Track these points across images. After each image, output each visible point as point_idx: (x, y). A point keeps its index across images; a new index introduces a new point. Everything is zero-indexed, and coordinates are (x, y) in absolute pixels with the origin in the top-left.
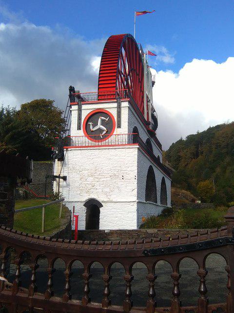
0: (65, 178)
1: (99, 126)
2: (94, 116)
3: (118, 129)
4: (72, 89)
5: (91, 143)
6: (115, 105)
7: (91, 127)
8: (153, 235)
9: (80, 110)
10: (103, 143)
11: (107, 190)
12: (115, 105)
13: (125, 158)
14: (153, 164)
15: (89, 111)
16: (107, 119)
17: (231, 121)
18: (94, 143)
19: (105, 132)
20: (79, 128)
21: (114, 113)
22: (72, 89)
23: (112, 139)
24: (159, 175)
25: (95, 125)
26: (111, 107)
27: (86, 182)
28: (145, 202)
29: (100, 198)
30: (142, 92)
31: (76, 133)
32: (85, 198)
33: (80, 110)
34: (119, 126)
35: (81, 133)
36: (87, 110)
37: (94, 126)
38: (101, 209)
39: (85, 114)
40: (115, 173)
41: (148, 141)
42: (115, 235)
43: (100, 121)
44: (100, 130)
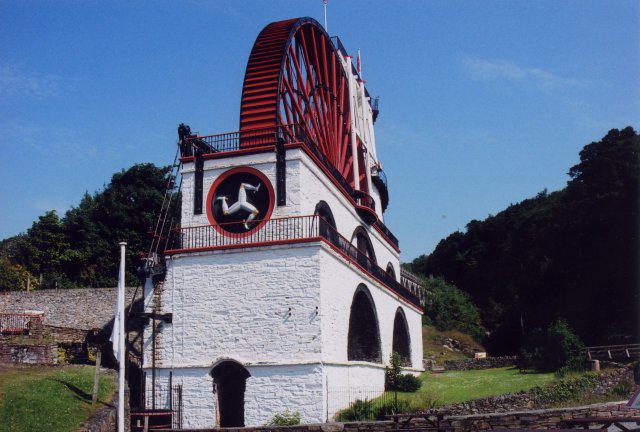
0: (168, 319)
1: (243, 201)
2: (228, 185)
3: (280, 209)
4: (183, 131)
5: (228, 240)
6: (272, 157)
10: (247, 240)
12: (272, 157)
13: (293, 268)
14: (366, 279)
15: (215, 177)
16: (257, 188)
18: (234, 241)
19: (252, 216)
20: (198, 211)
21: (270, 174)
22: (183, 131)
23: (267, 232)
24: (386, 305)
25: (233, 199)
26: (264, 163)
29: (242, 358)
30: (347, 132)
31: (194, 224)
32: (208, 361)
34: (282, 203)
35: (204, 219)
36: (214, 170)
38: (249, 381)
41: (361, 234)
43: (243, 194)
44: (244, 213)
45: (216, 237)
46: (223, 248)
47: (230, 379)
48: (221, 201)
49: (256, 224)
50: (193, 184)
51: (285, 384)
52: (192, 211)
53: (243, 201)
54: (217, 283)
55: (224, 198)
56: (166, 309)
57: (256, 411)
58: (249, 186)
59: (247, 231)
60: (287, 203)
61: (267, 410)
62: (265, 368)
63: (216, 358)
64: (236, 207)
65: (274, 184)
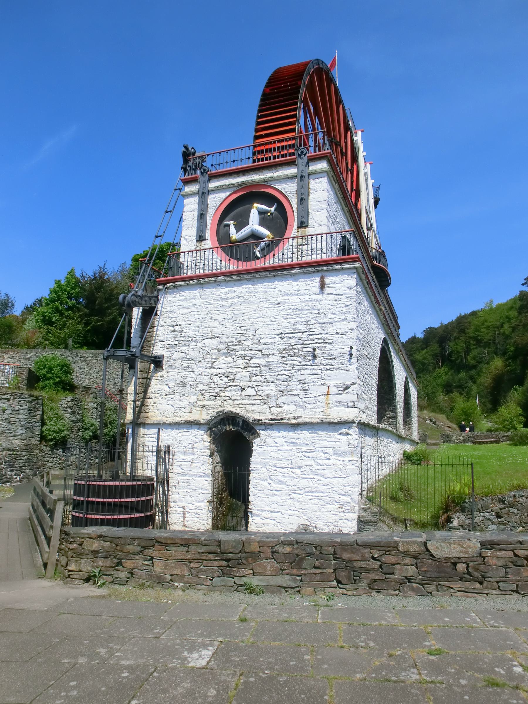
1: (254, 224)
4: (186, 147)
6: (292, 171)
7: (232, 230)
8: (461, 567)
9: (203, 195)
11: (271, 389)
16: (273, 209)
17: (502, 292)
20: (201, 238)
21: (289, 189)
27: (215, 371)
28: (373, 421)
33: (203, 195)
37: (238, 228)
39: (216, 201)
40: (293, 341)
42: (270, 565)
43: (254, 216)
44: (255, 237)
45: (218, 261)
46: (229, 274)
47: (233, 440)
48: (228, 226)
49: (272, 246)
50: (196, 206)
51: (304, 448)
52: (195, 238)
53: (254, 224)
54: (220, 317)
55: (232, 222)
56: (158, 350)
57: (265, 484)
58: (264, 207)
59: (258, 258)
60: (310, 223)
61: (281, 482)
62: (277, 424)
63: (216, 411)
64: (245, 231)
65: (294, 202)
